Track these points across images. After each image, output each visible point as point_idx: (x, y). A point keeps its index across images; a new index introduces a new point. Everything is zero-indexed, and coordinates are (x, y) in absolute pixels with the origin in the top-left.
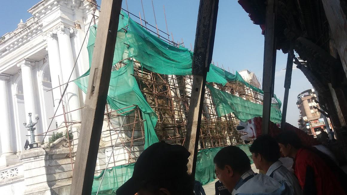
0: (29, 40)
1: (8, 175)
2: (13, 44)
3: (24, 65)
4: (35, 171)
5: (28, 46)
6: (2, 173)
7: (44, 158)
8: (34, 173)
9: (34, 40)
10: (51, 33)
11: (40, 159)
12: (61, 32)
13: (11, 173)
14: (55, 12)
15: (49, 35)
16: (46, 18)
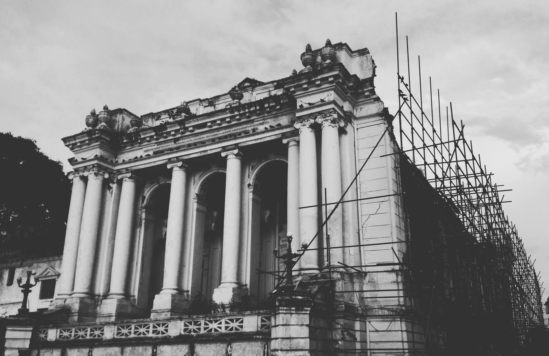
0: (253, 121)
1: (220, 326)
2: (223, 120)
3: (234, 156)
4: (293, 328)
5: (247, 129)
6: (207, 322)
7: (308, 312)
8: (294, 331)
9: (262, 122)
10: (312, 121)
11: (304, 312)
12: (330, 124)
13: (220, 326)
14: (323, 92)
15: (308, 124)
16: (305, 96)
